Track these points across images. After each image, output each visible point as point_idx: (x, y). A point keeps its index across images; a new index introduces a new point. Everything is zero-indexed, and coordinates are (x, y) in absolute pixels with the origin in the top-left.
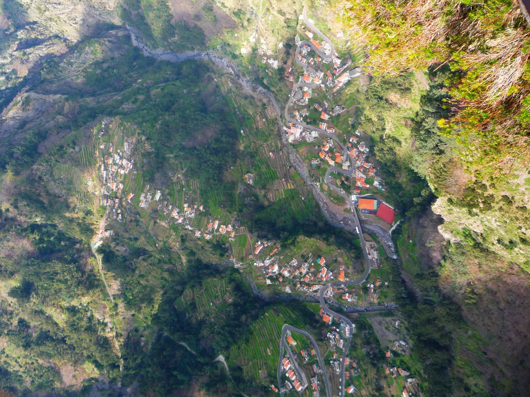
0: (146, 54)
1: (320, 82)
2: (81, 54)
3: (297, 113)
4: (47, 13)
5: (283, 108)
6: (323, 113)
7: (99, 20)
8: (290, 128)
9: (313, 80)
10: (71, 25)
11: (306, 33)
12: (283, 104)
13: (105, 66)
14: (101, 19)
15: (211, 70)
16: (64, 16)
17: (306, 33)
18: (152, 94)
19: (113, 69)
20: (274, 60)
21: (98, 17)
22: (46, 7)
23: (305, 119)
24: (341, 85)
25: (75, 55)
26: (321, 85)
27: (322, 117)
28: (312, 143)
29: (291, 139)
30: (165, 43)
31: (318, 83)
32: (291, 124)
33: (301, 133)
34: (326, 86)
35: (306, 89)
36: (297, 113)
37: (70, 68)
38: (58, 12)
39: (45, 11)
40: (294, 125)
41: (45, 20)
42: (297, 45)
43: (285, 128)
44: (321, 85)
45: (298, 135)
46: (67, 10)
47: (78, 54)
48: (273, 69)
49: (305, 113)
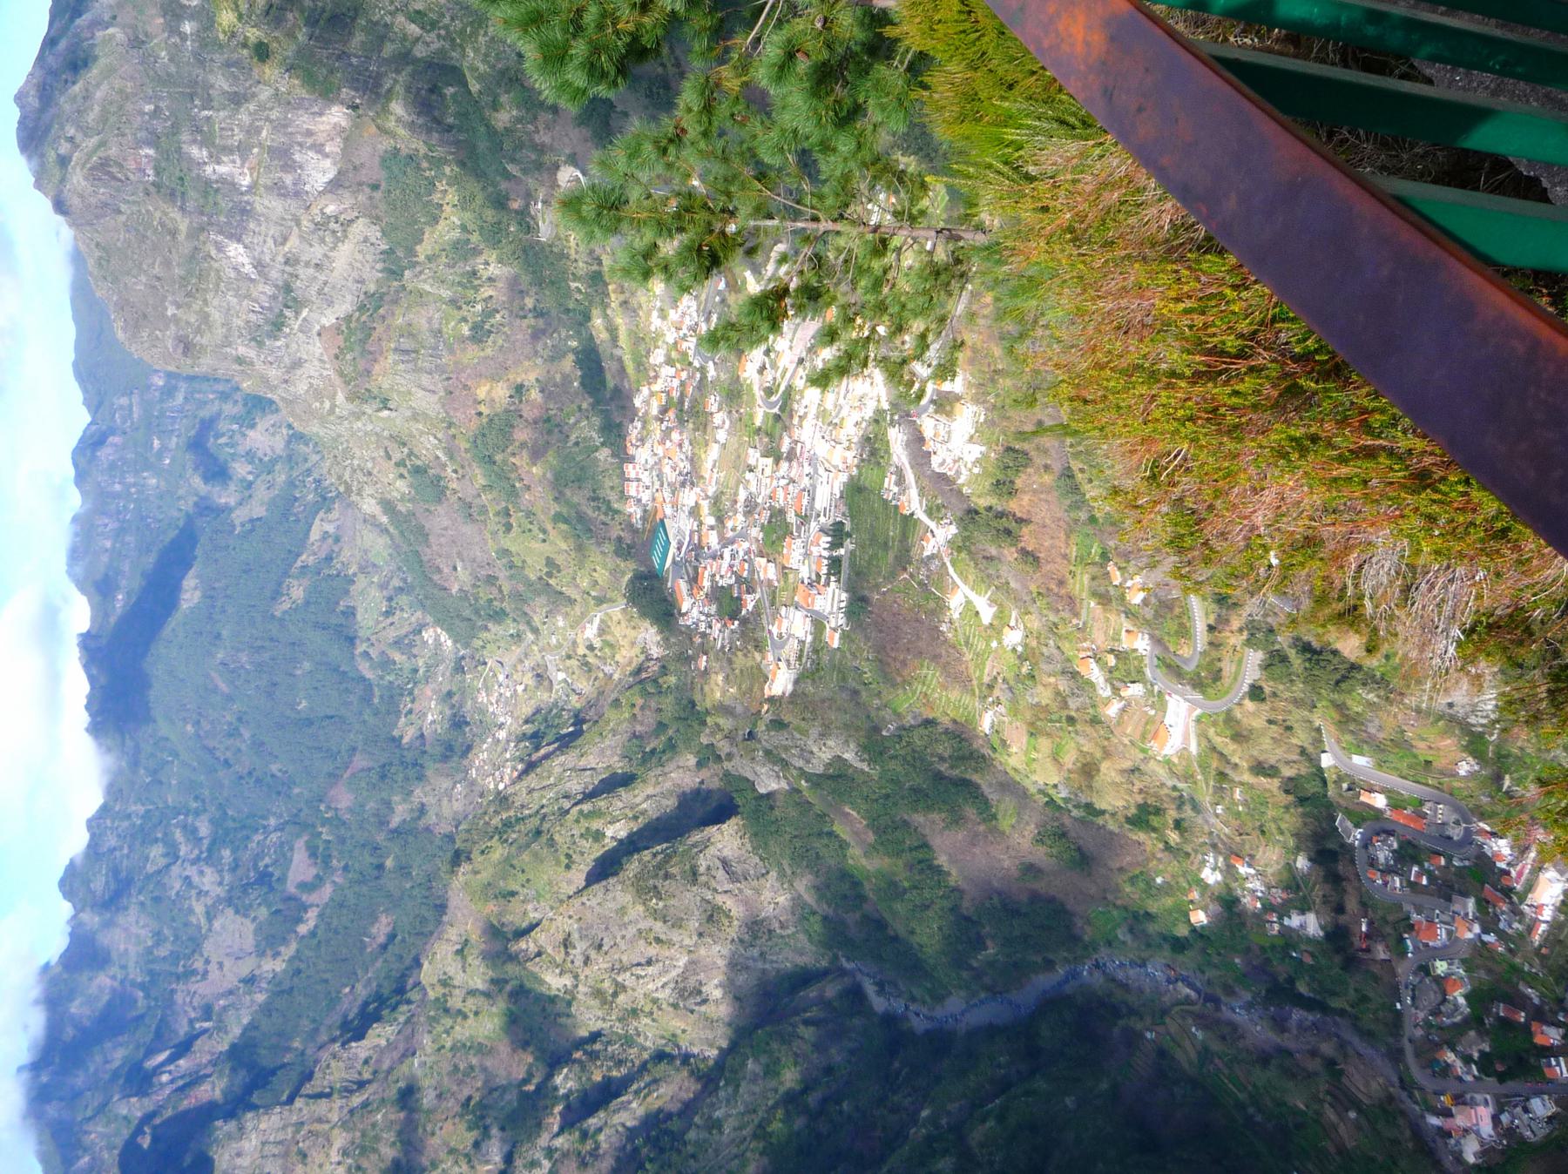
0: (919, 1025)
1: (1477, 929)
2: (738, 1086)
3: (1450, 1057)
4: (622, 998)
5: (1396, 1056)
6: (1535, 1026)
7: (764, 971)
8: (1447, 1114)
9: (1449, 933)
10: (692, 1012)
11: (1362, 798)
12: (1391, 1040)
13: (812, 1099)
14: (767, 966)
15: (1124, 1011)
16: (668, 991)
17: (1362, 798)
18: (973, 1144)
19: (838, 1103)
20: (1303, 912)
21: (760, 965)
22: (617, 984)
23: (1485, 1064)
24: (1547, 915)
25: (722, 1094)
26: (1486, 938)
27: (1539, 1040)
28: (1548, 1141)
29: (1470, 1151)
30: (965, 974)
31: (1469, 936)
32: (1445, 1099)
33: (1496, 1119)
34: (1502, 935)
35: (1441, 967)
36: (1450, 1057)
37: (717, 1138)
38: (651, 986)
39: (615, 994)
40: (1459, 1099)
41: (619, 1020)
42: (1352, 845)
43: (1434, 1121)
44: (1486, 938)
45: (1487, 1129)
46: (674, 973)
47: (730, 1090)
48: (1309, 940)
49: (1478, 1046)
